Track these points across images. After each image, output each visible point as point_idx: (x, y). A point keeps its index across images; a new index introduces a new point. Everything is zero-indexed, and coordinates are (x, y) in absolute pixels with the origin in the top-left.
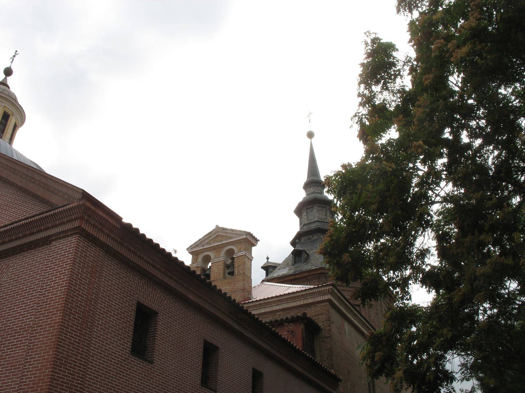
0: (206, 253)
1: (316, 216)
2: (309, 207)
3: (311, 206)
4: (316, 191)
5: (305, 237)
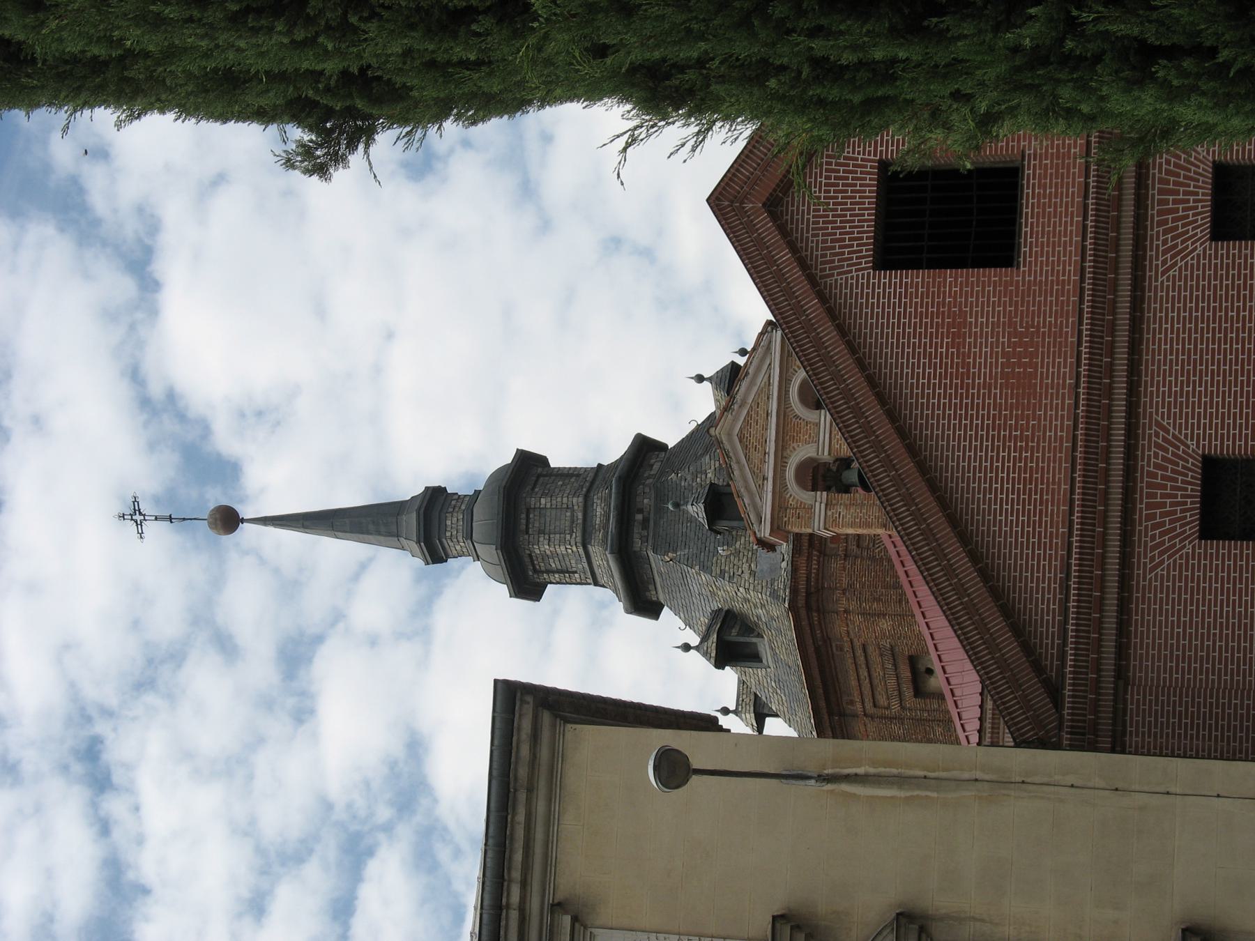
0: (790, 474)
1: (565, 500)
2: (524, 521)
3: (523, 516)
4: (463, 507)
5: (636, 536)
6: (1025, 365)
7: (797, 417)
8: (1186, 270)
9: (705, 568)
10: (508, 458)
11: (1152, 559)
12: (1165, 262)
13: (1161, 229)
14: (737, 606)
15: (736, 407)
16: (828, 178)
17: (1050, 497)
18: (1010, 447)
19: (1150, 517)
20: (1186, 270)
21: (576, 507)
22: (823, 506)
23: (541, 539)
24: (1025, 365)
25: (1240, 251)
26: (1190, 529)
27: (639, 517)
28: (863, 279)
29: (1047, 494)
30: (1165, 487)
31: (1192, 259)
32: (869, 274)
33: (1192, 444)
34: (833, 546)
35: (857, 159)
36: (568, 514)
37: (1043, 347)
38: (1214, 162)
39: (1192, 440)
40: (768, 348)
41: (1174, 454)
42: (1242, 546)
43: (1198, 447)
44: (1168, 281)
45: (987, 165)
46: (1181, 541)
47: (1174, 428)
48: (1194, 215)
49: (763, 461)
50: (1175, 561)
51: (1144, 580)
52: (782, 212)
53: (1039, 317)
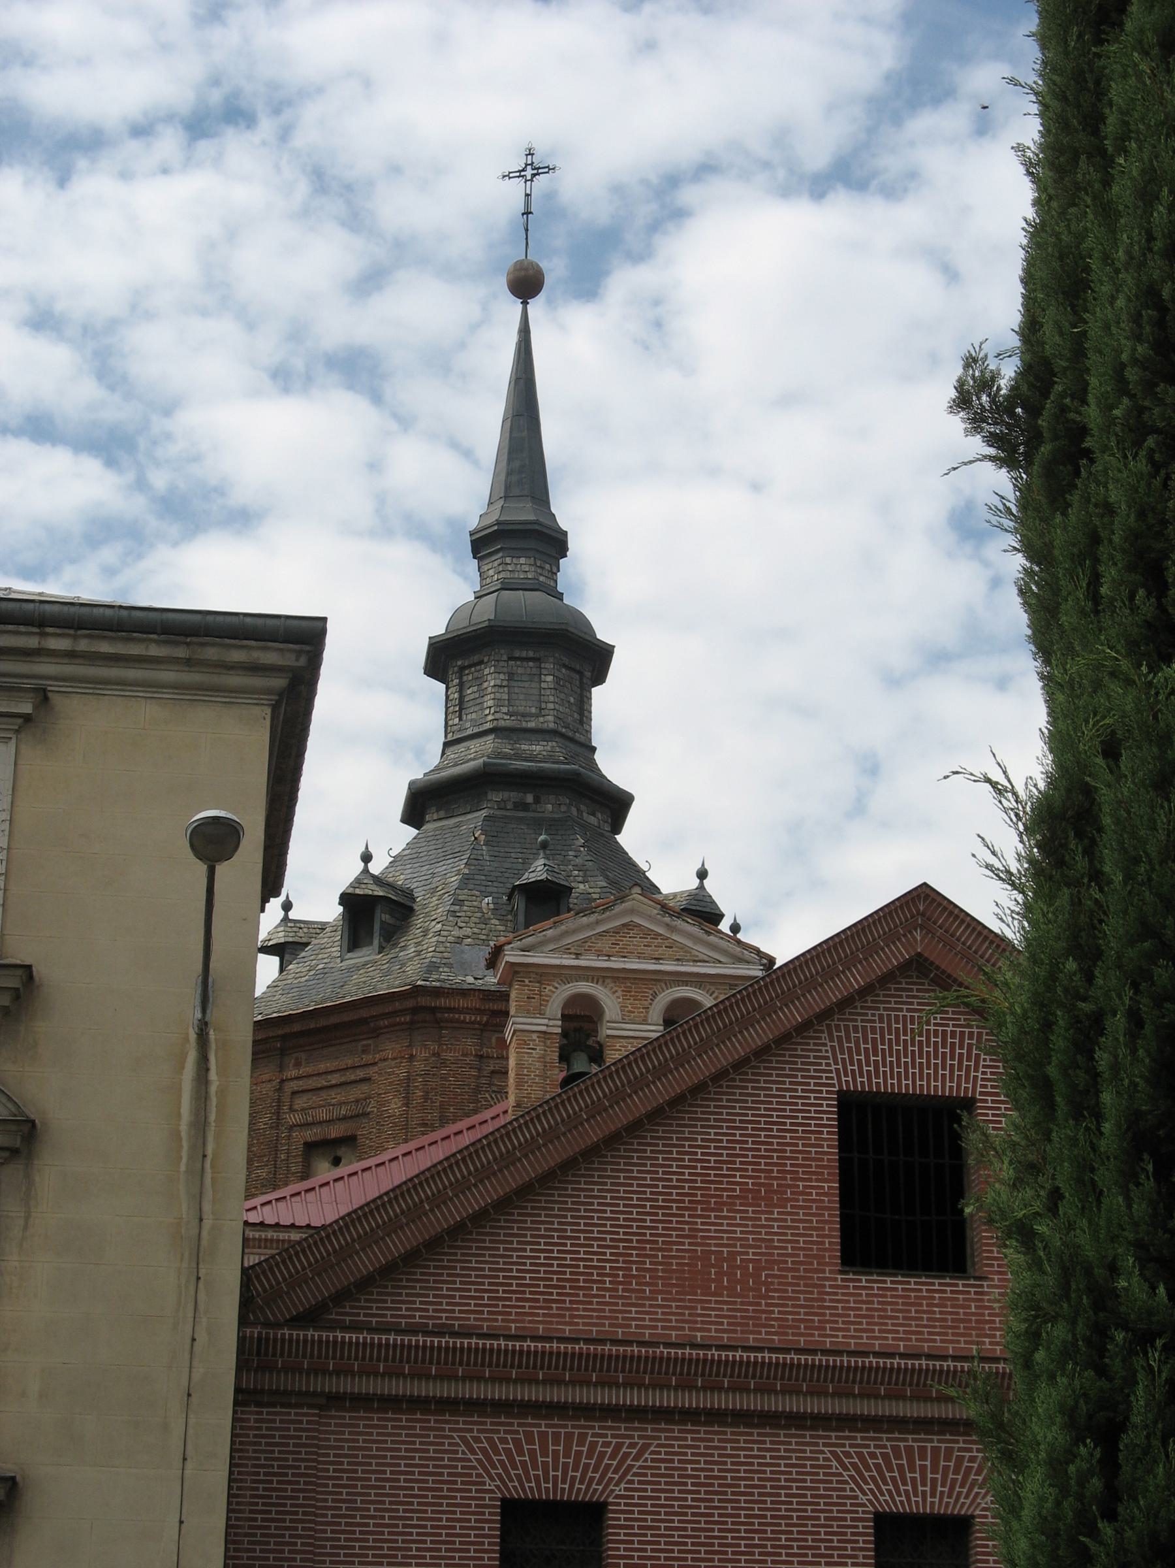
0: (584, 987)
1: (551, 706)
2: (524, 654)
3: (531, 654)
6: (718, 1281)
7: (655, 995)
8: (838, 1482)
9: (466, 881)
10: (603, 634)
11: (477, 1440)
12: (848, 1455)
13: (889, 1451)
14: (418, 921)
15: (667, 919)
16: (953, 1034)
17: (555, 1311)
18: (617, 1261)
19: (530, 1438)
20: (838, 1482)
21: (541, 719)
22: (543, 1028)
23: (502, 676)
24: (718, 1281)
25: (861, 1549)
26: (514, 1487)
27: (530, 798)
28: (827, 1078)
29: (558, 1308)
30: (567, 1455)
31: (852, 1490)
32: (833, 1085)
33: (620, 1490)
34: (494, 1040)
35: (976, 1070)
36: (533, 710)
37: (742, 1303)
38: (973, 1517)
39: (626, 1489)
40: (740, 960)
41: (608, 1466)
42: (494, 1551)
43: (617, 1497)
44: (825, 1459)
45: (968, 1232)
46: (499, 1475)
47: (640, 1467)
48: (906, 1491)
49: (599, 954)
50: (474, 1468)
51: (451, 1430)
52: (911, 977)
53: (779, 1298)
